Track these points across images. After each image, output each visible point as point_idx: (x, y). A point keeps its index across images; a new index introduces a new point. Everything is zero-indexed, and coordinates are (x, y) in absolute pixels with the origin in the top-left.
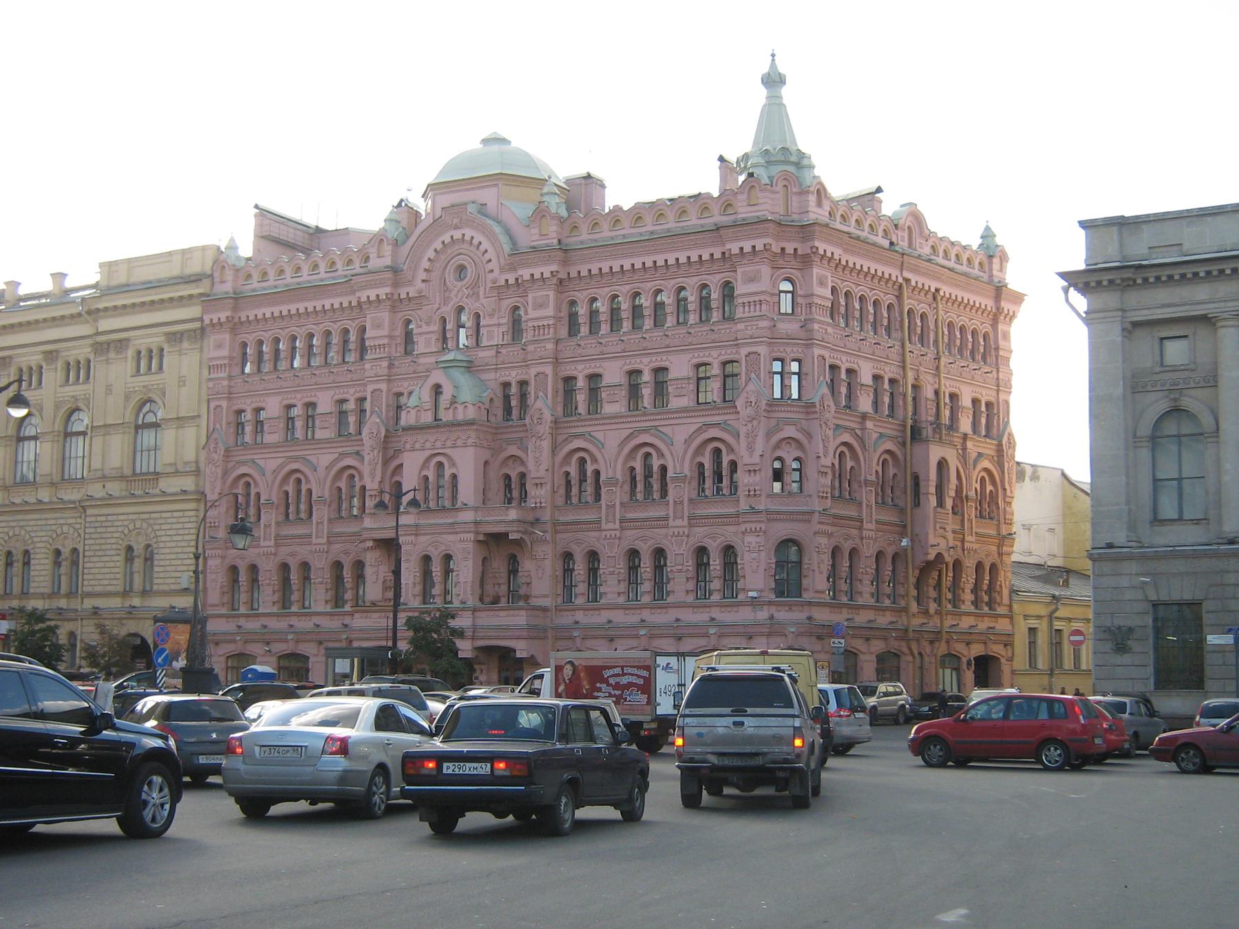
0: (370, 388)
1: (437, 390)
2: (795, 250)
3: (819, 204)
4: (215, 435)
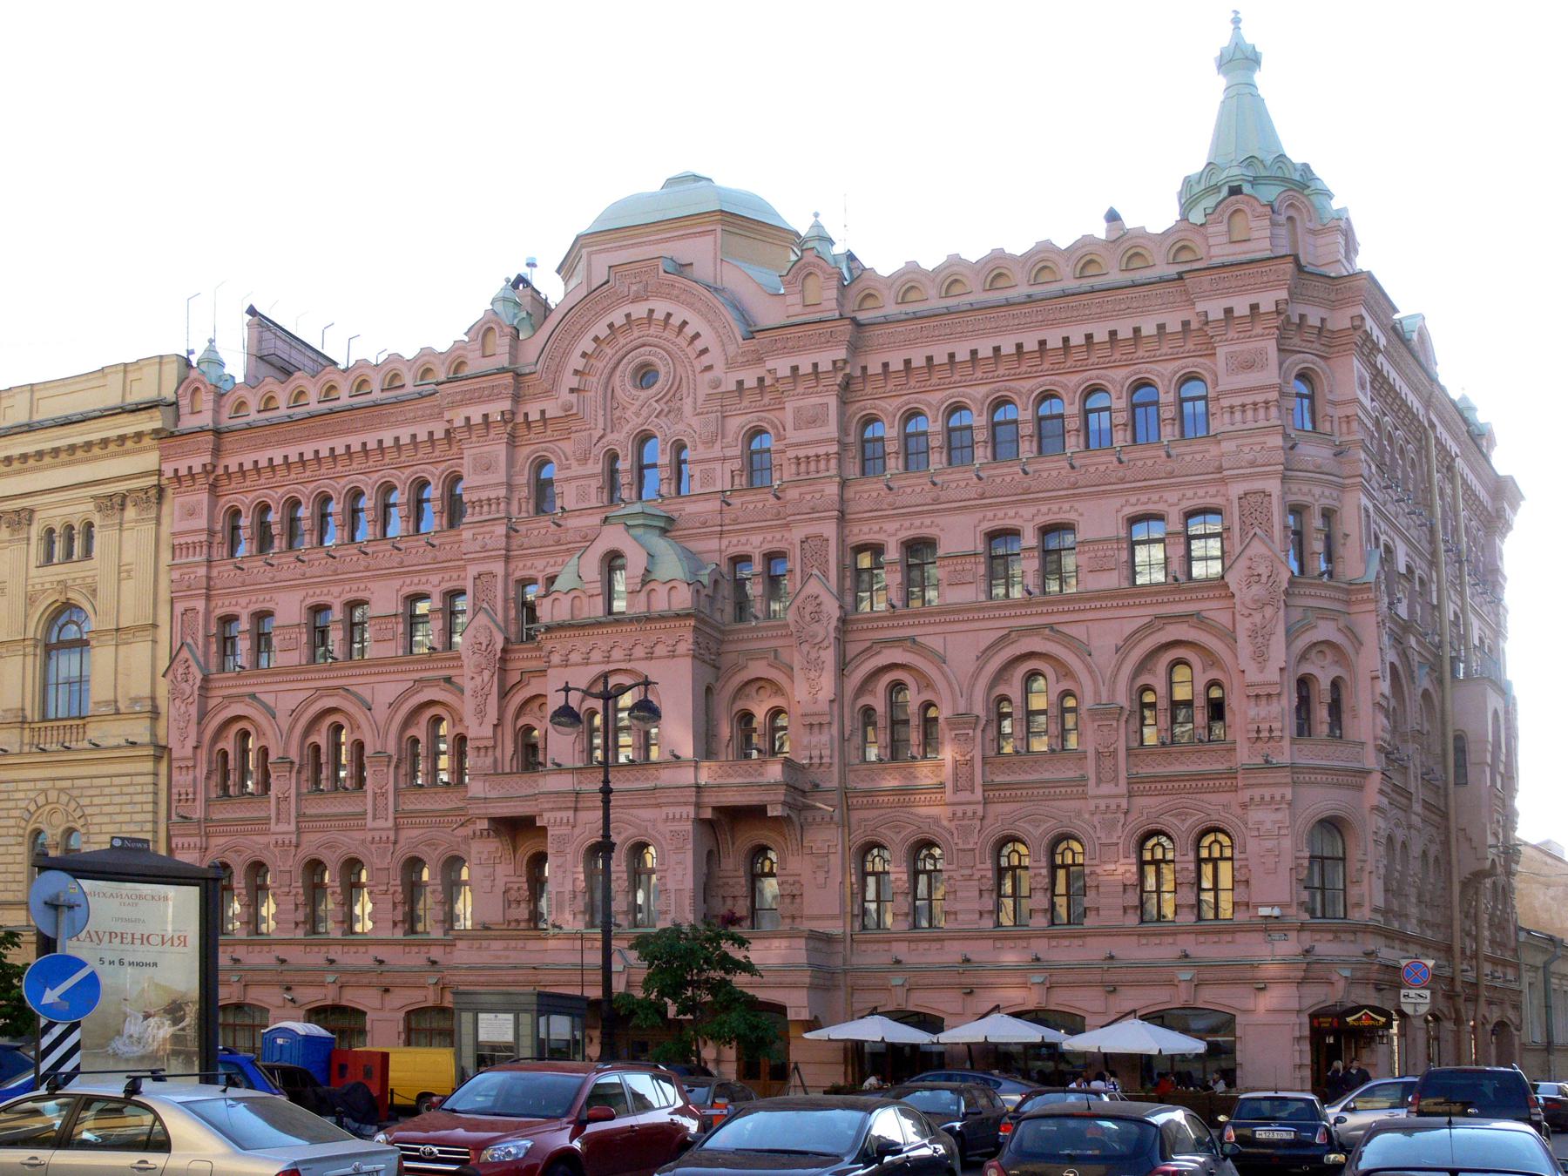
0: (473, 570)
4: (185, 654)
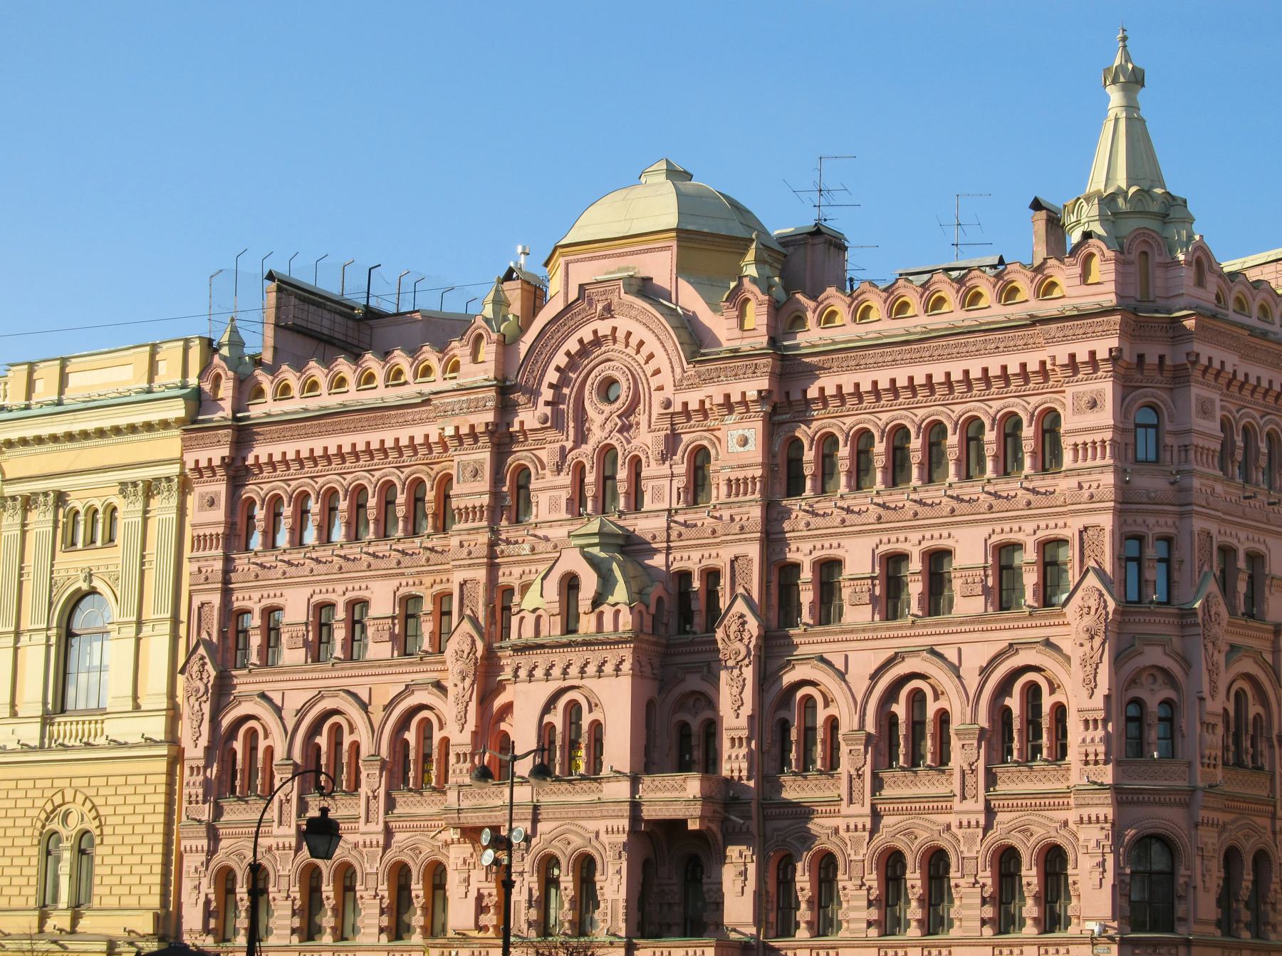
0: (458, 577)
1: (570, 584)
2: (1162, 358)
3: (1200, 282)
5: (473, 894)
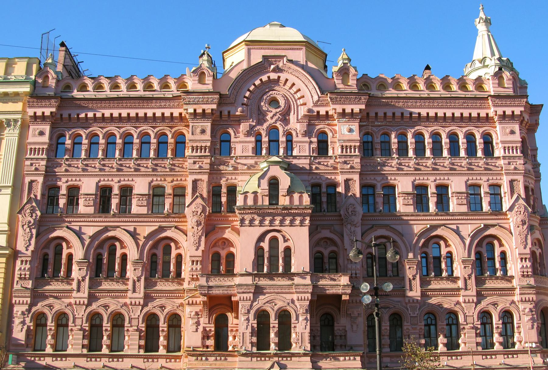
5: (201, 329)
